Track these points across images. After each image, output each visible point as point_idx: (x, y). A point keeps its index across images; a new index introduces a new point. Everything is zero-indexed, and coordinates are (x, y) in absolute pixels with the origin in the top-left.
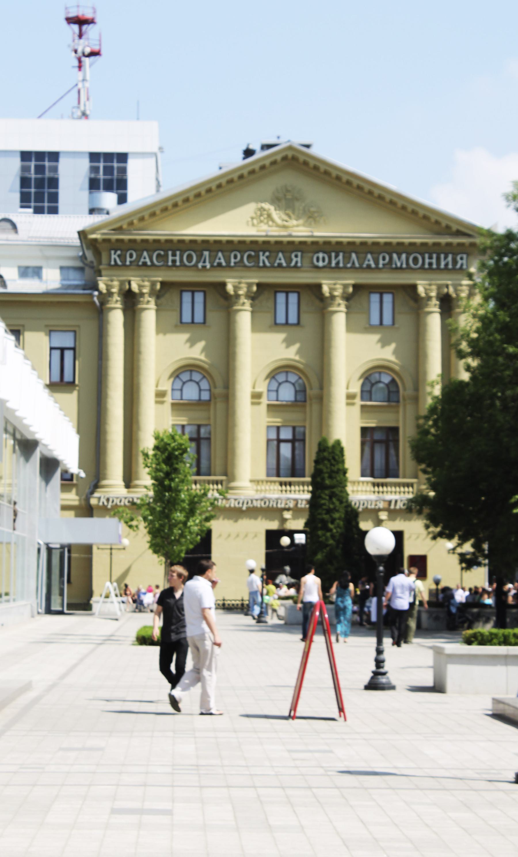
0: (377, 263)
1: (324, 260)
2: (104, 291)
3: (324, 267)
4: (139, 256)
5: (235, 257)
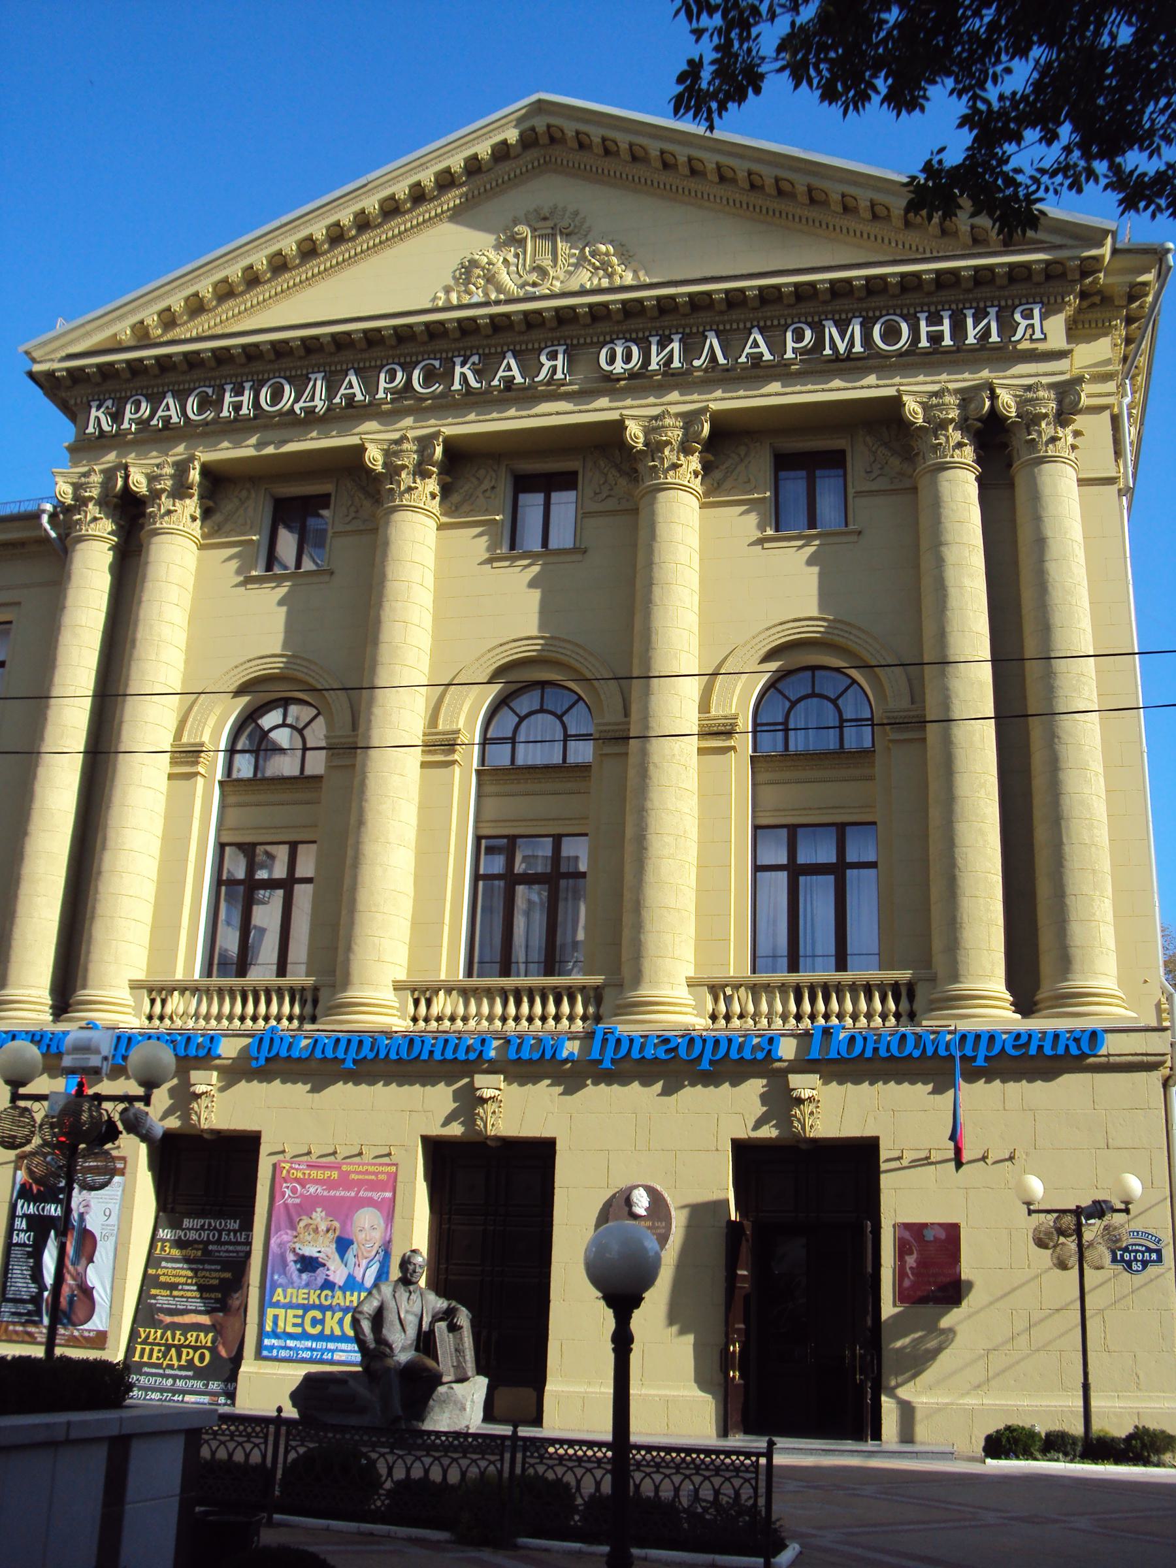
0: (777, 347)
1: (628, 358)
3: (632, 376)
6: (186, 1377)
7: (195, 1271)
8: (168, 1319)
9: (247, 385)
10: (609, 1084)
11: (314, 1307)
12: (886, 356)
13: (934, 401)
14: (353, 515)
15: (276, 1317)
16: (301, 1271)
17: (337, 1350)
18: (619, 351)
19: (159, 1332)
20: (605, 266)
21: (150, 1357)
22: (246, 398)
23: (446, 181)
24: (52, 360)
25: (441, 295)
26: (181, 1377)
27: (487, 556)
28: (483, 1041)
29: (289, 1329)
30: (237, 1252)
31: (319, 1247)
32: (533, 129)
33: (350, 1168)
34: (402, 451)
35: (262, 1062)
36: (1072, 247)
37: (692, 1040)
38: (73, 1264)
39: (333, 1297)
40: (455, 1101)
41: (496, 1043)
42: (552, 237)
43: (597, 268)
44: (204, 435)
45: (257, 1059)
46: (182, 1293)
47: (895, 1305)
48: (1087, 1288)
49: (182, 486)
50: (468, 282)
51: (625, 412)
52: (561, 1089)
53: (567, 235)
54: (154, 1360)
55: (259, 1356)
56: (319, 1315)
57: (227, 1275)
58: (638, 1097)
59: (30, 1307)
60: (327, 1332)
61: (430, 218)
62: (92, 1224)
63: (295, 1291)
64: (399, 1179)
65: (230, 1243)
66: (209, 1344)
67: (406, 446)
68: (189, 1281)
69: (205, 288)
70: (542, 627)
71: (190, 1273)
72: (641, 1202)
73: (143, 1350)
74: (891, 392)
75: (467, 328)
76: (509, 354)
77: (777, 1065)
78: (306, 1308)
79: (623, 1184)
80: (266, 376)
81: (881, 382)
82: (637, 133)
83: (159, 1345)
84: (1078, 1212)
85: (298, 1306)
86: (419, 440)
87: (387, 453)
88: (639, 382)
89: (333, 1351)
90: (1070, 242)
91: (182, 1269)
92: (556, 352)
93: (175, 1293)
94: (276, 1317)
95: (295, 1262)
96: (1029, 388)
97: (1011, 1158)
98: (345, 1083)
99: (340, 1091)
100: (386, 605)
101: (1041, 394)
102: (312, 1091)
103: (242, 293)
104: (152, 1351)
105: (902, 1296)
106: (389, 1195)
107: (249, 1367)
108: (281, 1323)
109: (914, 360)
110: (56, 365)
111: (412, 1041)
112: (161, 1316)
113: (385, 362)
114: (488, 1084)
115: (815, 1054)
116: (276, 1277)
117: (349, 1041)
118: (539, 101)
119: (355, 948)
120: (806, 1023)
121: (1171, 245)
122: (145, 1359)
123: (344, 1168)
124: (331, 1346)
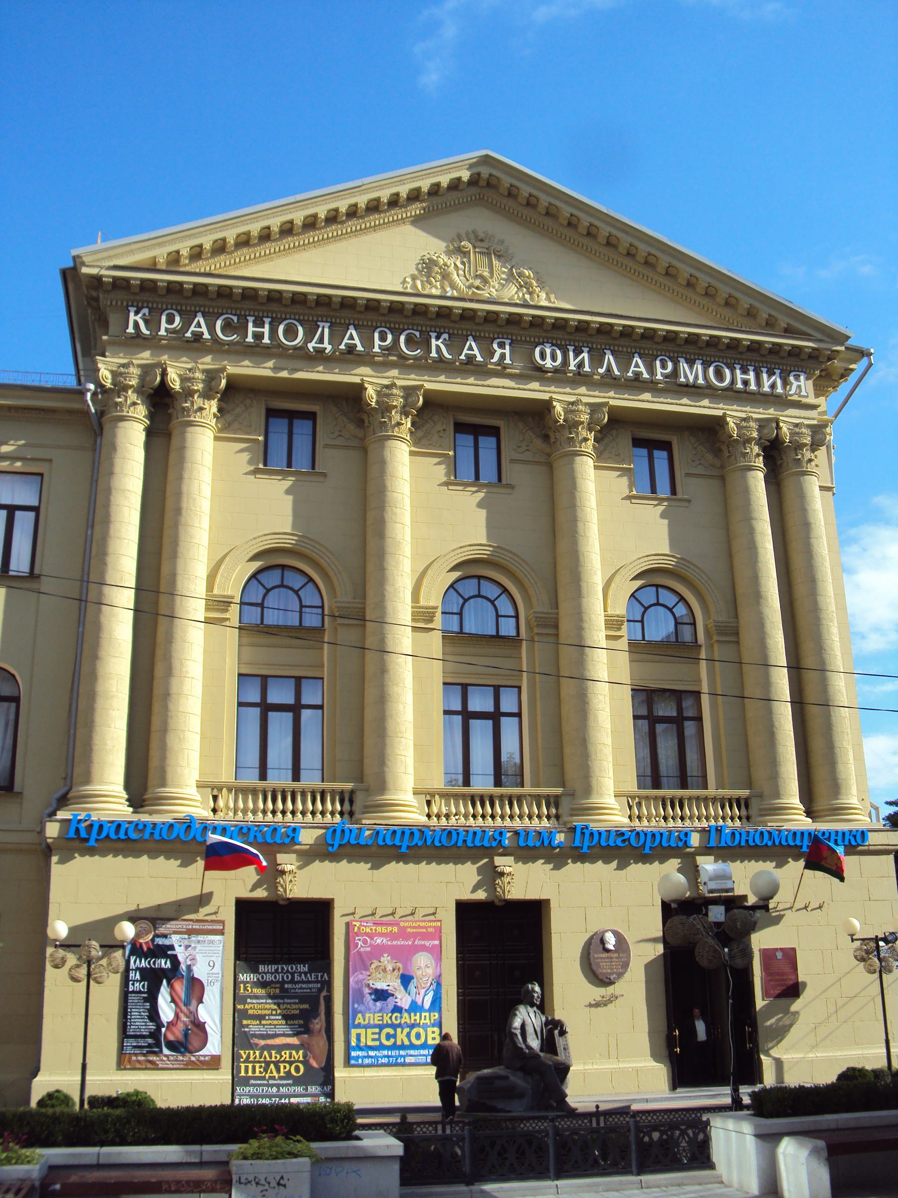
0: (651, 370)
1: (554, 358)
2: (108, 384)
3: (556, 371)
4: (186, 324)
5: (383, 338)
6: (287, 1085)
7: (278, 1005)
8: (262, 1042)
9: (267, 320)
10: (583, 862)
11: (387, 1026)
12: (716, 389)
13: (744, 424)
14: (337, 433)
15: (358, 1035)
16: (375, 1000)
17: (408, 1055)
18: (548, 351)
19: (257, 1053)
20: (528, 286)
21: (254, 1071)
22: (266, 330)
23: (415, 196)
24: (102, 268)
25: (409, 280)
26: (283, 1085)
27: (445, 479)
28: (501, 833)
29: (370, 1043)
30: (310, 989)
31: (388, 982)
32: (479, 174)
33: (406, 924)
34: (392, 394)
35: (336, 846)
36: (827, 342)
37: (638, 834)
38: (186, 1005)
39: (401, 1017)
40: (479, 875)
41: (509, 835)
42: (488, 254)
43: (521, 286)
44: (228, 352)
45: (332, 845)
46: (269, 1022)
47: (763, 1000)
48: (878, 981)
49: (211, 389)
50: (429, 275)
51: (554, 396)
52: (551, 866)
53: (499, 257)
54: (257, 1074)
55: (348, 1063)
56: (391, 1031)
57: (306, 1006)
58: (601, 870)
59: (150, 1041)
60: (399, 1043)
61: (398, 220)
62: (199, 972)
63: (372, 1015)
64: (443, 931)
65: (303, 982)
66: (301, 1059)
67: (395, 391)
68: (274, 1012)
69: (231, 235)
70: (489, 536)
71: (276, 1007)
72: (611, 941)
73: (247, 1067)
74: (719, 413)
75: (444, 314)
76: (470, 338)
77: (688, 850)
78: (381, 1027)
79: (593, 929)
80: (283, 316)
81: (711, 405)
82: (556, 198)
83: (259, 1062)
84: (876, 940)
85: (375, 1026)
86: (405, 388)
87: (378, 393)
88: (559, 376)
89: (404, 1057)
90: (826, 339)
91: (266, 1003)
92: (504, 343)
93: (263, 1022)
94: (358, 1035)
95: (370, 994)
96: (797, 425)
97: (820, 907)
98: (398, 862)
99: (394, 869)
100: (388, 509)
101: (804, 430)
102: (372, 868)
103: (255, 245)
104: (254, 1068)
105: (766, 994)
106: (437, 942)
107: (340, 1073)
108: (363, 1039)
109: (733, 394)
110: (104, 272)
111: (450, 832)
112: (256, 1041)
113: (379, 325)
114: (504, 863)
115: (712, 844)
116: (356, 1006)
117: (403, 833)
118: (487, 156)
119: (389, 763)
120: (705, 824)
121: (872, 351)
122: (250, 1074)
123: (402, 924)
124: (402, 1053)
